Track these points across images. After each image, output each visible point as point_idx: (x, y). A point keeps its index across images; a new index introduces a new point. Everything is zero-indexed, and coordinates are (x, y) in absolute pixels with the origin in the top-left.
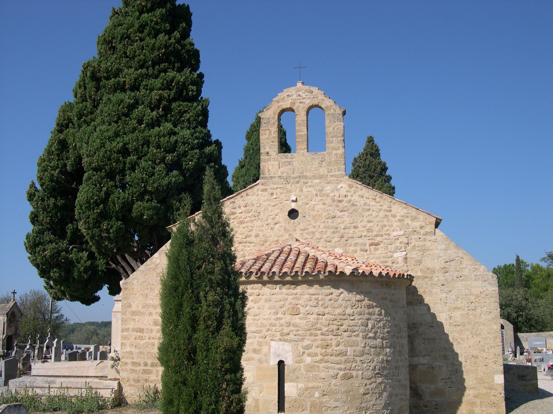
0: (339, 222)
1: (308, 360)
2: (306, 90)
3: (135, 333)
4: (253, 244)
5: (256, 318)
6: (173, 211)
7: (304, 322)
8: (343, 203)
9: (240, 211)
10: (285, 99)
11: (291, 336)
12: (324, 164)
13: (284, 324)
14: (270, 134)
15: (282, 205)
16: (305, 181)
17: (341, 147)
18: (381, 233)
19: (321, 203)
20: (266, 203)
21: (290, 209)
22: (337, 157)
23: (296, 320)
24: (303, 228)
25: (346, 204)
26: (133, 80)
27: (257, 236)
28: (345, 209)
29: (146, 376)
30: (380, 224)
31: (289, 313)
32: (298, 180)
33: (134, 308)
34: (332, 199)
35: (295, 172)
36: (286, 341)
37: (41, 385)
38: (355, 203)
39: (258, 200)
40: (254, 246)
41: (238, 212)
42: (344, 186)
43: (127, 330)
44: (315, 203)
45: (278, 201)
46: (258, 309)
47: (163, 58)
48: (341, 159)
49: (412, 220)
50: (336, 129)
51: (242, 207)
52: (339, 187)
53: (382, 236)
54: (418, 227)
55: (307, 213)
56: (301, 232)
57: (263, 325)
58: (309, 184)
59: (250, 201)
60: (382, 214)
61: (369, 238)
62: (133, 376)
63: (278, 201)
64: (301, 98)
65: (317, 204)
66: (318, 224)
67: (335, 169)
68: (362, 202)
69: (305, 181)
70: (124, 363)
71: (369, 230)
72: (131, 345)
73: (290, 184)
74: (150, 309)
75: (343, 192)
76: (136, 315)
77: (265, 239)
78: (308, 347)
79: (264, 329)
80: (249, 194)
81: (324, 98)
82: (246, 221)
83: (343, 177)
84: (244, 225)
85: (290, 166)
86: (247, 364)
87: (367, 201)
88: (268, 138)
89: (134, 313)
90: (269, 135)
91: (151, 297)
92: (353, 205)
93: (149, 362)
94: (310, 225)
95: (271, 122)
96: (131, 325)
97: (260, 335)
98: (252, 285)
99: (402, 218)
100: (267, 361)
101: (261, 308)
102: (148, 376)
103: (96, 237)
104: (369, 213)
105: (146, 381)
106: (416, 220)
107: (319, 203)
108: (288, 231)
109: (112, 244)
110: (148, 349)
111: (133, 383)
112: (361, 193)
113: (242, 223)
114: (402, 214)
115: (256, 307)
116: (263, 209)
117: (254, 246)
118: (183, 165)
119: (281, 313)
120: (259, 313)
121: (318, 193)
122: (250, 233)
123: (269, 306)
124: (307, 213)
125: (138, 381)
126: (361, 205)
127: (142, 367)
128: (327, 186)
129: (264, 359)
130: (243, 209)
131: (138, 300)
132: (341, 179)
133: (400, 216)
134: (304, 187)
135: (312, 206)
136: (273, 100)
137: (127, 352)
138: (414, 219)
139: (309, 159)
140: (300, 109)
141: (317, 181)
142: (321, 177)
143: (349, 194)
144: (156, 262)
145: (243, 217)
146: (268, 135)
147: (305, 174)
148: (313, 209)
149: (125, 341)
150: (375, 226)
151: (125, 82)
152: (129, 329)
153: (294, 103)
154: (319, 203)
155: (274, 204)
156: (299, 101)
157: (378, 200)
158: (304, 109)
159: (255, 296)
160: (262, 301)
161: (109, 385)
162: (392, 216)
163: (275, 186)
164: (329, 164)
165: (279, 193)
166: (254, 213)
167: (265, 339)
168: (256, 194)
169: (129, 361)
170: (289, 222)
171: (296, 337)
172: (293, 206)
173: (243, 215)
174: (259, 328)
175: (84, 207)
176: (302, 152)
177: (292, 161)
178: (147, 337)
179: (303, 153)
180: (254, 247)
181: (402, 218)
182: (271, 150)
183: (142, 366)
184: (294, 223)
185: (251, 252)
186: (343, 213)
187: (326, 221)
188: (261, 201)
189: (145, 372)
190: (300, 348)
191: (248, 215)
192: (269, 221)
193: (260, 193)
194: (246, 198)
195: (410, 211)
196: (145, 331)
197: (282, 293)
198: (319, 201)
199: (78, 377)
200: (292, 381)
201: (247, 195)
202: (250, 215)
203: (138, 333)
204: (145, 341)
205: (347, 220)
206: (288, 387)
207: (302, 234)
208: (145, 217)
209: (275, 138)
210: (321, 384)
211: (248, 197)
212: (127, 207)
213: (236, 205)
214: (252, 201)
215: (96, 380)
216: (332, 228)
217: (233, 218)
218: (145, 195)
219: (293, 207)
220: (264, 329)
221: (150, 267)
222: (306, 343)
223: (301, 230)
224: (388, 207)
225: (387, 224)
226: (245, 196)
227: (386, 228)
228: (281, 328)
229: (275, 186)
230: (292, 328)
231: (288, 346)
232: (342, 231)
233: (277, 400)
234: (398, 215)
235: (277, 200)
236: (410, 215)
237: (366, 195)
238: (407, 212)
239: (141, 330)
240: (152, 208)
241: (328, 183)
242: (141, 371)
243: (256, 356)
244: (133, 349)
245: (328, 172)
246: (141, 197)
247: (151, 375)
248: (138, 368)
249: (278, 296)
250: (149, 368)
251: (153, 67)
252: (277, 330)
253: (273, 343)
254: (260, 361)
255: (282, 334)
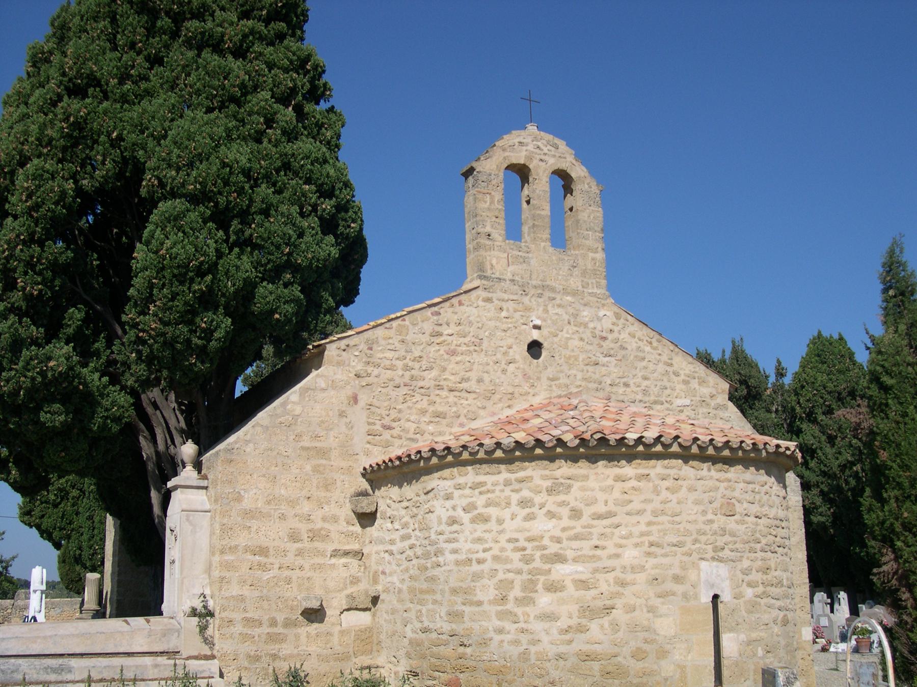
0: (603, 373)
1: (749, 592)
2: (548, 142)
3: (250, 557)
4: (474, 395)
5: (677, 519)
6: (318, 313)
7: (742, 528)
8: (607, 342)
9: (450, 332)
10: (515, 147)
11: (726, 553)
12: (577, 273)
13: (718, 532)
14: (492, 202)
15: (517, 331)
16: (552, 295)
17: (600, 249)
18: (660, 399)
19: (576, 336)
20: (492, 324)
21: (531, 340)
22: (595, 263)
23: (731, 524)
24: (551, 376)
25: (612, 345)
26: (240, 37)
27: (480, 381)
28: (612, 352)
29: (273, 648)
30: (659, 384)
31: (723, 512)
32: (540, 291)
33: (247, 504)
34: (592, 332)
35: (534, 277)
36: (720, 560)
37: (35, 676)
38: (625, 345)
39: (479, 316)
40: (474, 399)
41: (446, 332)
42: (608, 313)
43: (233, 549)
44: (569, 336)
45: (511, 323)
46: (678, 503)
47: (281, 10)
48: (601, 269)
49: (700, 384)
50: (592, 217)
51: (452, 325)
52: (601, 313)
53: (662, 404)
54: (707, 396)
55: (557, 350)
56: (549, 383)
57: (687, 533)
58: (558, 301)
59: (465, 315)
60: (661, 368)
61: (645, 405)
62: (248, 648)
63: (511, 323)
64: (542, 153)
65: (571, 338)
66: (574, 372)
67: (592, 283)
68: (634, 345)
69: (552, 295)
70: (226, 620)
71: (645, 392)
72: (242, 582)
73: (528, 297)
74: (283, 507)
75: (607, 324)
76: (253, 518)
77: (493, 388)
78: (746, 572)
79: (689, 540)
80: (463, 302)
81: (574, 162)
82: (460, 352)
83: (606, 299)
84: (458, 358)
85: (525, 265)
86: (663, 603)
87: (640, 343)
88: (489, 209)
89: (248, 514)
90: (490, 203)
91: (283, 481)
92: (623, 348)
93: (280, 618)
94: (562, 372)
95: (494, 182)
96: (242, 539)
97: (684, 549)
98: (666, 461)
99: (687, 378)
100: (696, 597)
101: (683, 503)
102: (277, 646)
103: (178, 343)
104: (644, 363)
105: (275, 657)
106: (705, 384)
107: (573, 336)
108: (529, 378)
109: (203, 363)
110: (278, 589)
111: (246, 664)
112: (631, 329)
113: (453, 353)
114: (687, 372)
115: (675, 501)
116: (487, 334)
117: (474, 399)
118: (339, 225)
119: (711, 511)
120: (679, 510)
121: (572, 320)
122: (468, 374)
123: (696, 499)
124: (557, 350)
125: (257, 658)
126: (632, 350)
127: (265, 629)
128: (584, 311)
129: (691, 593)
130: (452, 329)
131: (257, 488)
132: (603, 302)
133: (685, 375)
134: (550, 305)
135: (563, 339)
136: (497, 144)
137: (233, 597)
138: (702, 382)
139: (554, 258)
140: (541, 172)
141: (569, 298)
142: (574, 293)
143: (616, 329)
144: (293, 410)
145: (455, 342)
146: (488, 204)
147: (548, 283)
148: (566, 347)
149: (228, 575)
150: (653, 387)
151: (223, 35)
152: (236, 547)
153: (530, 158)
154: (573, 336)
155: (505, 326)
156: (538, 157)
157: (655, 344)
158: (547, 172)
159: (672, 481)
160: (684, 489)
161: (201, 669)
162: (674, 373)
163: (506, 296)
164: (584, 273)
165: (511, 309)
166: (473, 339)
167: (691, 558)
168: (475, 305)
169: (237, 616)
170: (530, 362)
171: (733, 553)
172: (535, 335)
173: (455, 340)
174: (681, 538)
175: (167, 273)
176: (543, 244)
177: (528, 258)
178: (277, 566)
179: (544, 247)
180: (475, 401)
181: (687, 378)
182: (494, 231)
183: (265, 626)
184: (538, 366)
185: (469, 409)
186: (607, 359)
187: (585, 368)
188: (484, 319)
189: (272, 638)
190: (738, 573)
191: (462, 340)
192: (499, 356)
193: (481, 303)
194: (458, 308)
195: (697, 369)
196: (272, 552)
197: (711, 478)
198: (573, 334)
199: (82, 655)
200: (731, 630)
201: (460, 304)
202: (466, 340)
203: (257, 557)
204: (271, 574)
205: (616, 371)
206: (726, 640)
207: (550, 386)
208: (277, 316)
209: (500, 210)
210: (763, 634)
211: (461, 307)
212: (247, 292)
213: (443, 319)
214: (469, 317)
215: (148, 660)
216: (595, 382)
217: (438, 341)
218: (284, 272)
219: (535, 338)
220: (689, 540)
221: (282, 419)
222: (746, 563)
223: (549, 379)
224: (669, 359)
225: (668, 385)
226: (457, 305)
227: (668, 392)
228: (713, 537)
229: (506, 296)
230: (727, 538)
231: (723, 570)
232: (608, 389)
233: (713, 664)
234: (682, 372)
235: (509, 320)
236: (696, 375)
237: (639, 334)
238: (693, 370)
239: (263, 551)
240: (292, 301)
241: (585, 305)
242: (264, 637)
243: (679, 589)
244: (246, 591)
245: (583, 287)
246: (273, 275)
247: (284, 646)
248: (257, 631)
249: (706, 482)
250: (279, 630)
251: (267, 21)
252: (708, 542)
253: (703, 564)
254: (685, 596)
255: (716, 549)
